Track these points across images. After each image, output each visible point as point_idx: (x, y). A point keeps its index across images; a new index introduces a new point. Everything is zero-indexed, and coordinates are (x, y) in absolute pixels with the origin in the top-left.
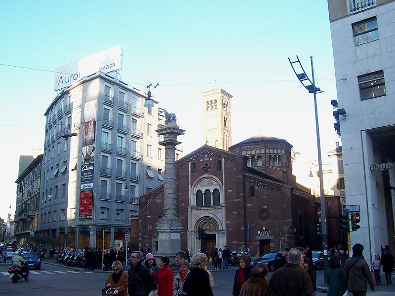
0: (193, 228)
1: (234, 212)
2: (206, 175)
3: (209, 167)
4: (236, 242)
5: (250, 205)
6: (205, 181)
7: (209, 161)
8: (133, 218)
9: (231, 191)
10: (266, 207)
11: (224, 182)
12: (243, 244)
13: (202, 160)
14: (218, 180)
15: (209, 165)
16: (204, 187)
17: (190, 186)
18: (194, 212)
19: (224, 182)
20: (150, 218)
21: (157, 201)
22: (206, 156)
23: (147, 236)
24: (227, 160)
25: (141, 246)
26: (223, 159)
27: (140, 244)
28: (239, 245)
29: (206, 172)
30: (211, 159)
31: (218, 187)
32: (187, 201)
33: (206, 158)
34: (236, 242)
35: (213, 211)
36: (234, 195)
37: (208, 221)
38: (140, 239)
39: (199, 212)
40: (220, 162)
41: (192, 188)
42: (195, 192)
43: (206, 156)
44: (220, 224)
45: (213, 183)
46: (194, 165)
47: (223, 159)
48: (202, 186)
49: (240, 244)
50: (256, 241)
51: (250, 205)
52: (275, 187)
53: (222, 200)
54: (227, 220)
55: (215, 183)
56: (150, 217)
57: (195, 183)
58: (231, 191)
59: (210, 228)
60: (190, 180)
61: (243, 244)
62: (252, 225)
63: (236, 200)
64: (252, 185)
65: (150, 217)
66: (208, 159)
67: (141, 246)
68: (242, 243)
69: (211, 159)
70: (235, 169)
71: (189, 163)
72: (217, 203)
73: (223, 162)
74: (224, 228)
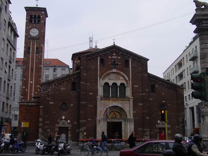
0: (102, 117)
1: (139, 104)
2: (114, 70)
3: (117, 64)
4: (141, 129)
5: (151, 99)
6: (112, 76)
7: (117, 59)
8: (22, 104)
9: (137, 86)
10: (164, 102)
11: (131, 78)
12: (148, 131)
13: (110, 57)
14: (126, 76)
15: (118, 62)
16: (111, 81)
17: (99, 78)
18: (103, 101)
19: (131, 78)
20: (52, 104)
21: (61, 89)
22: (114, 54)
23: (49, 122)
24: (133, 60)
25: (42, 131)
26: (130, 59)
27: (40, 129)
28: (144, 132)
29: (115, 68)
30: (119, 58)
31: (124, 82)
32: (96, 92)
33: (114, 56)
34: (141, 129)
35: (122, 102)
36: (140, 90)
37: (115, 110)
38: (41, 124)
39: (107, 101)
40: (127, 62)
41: (101, 80)
42: (103, 84)
43: (114, 54)
44: (128, 113)
45: (120, 77)
46: (102, 61)
47: (130, 59)
48: (109, 79)
49: (145, 130)
50: (156, 128)
51: (151, 99)
52: (171, 87)
53: (129, 92)
54: (134, 110)
55: (121, 78)
56: (52, 103)
57: (103, 76)
58: (137, 86)
59: (116, 116)
60: (99, 73)
61: (148, 131)
62: (153, 115)
63: (141, 94)
64: (153, 83)
65: (52, 103)
66: (116, 57)
67: (42, 131)
68: (147, 130)
69: (119, 58)
70: (140, 69)
71: (99, 58)
72: (123, 96)
73: (130, 62)
74: (132, 117)
